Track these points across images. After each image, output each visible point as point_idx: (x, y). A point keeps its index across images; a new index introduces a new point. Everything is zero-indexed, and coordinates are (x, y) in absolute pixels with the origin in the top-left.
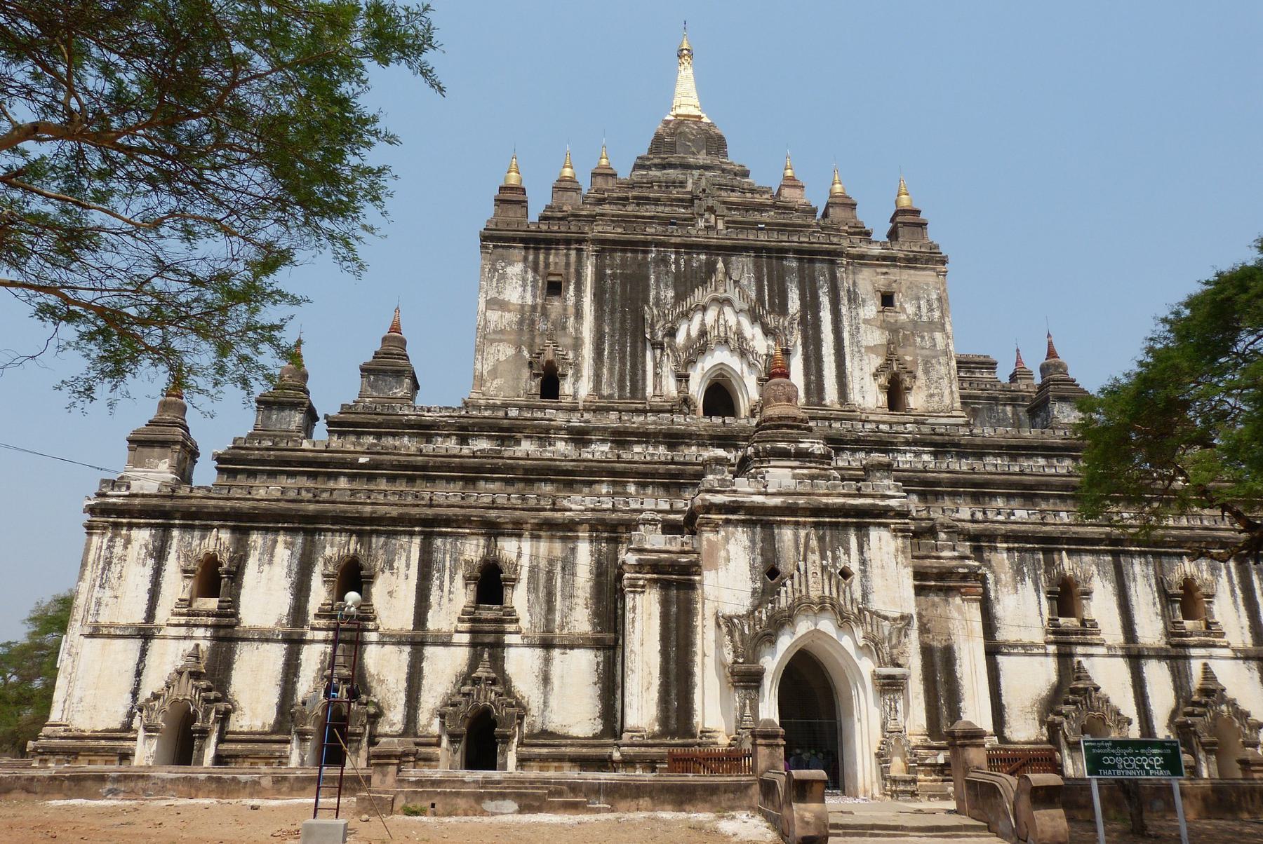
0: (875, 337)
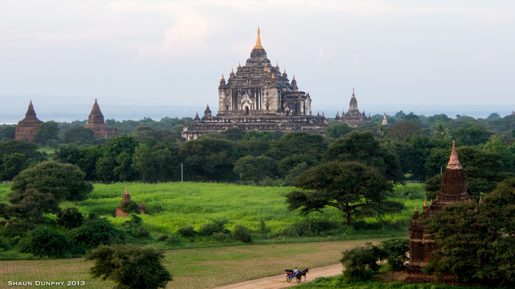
0: (265, 100)
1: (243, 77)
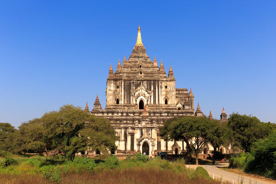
0: (164, 93)
1: (131, 70)
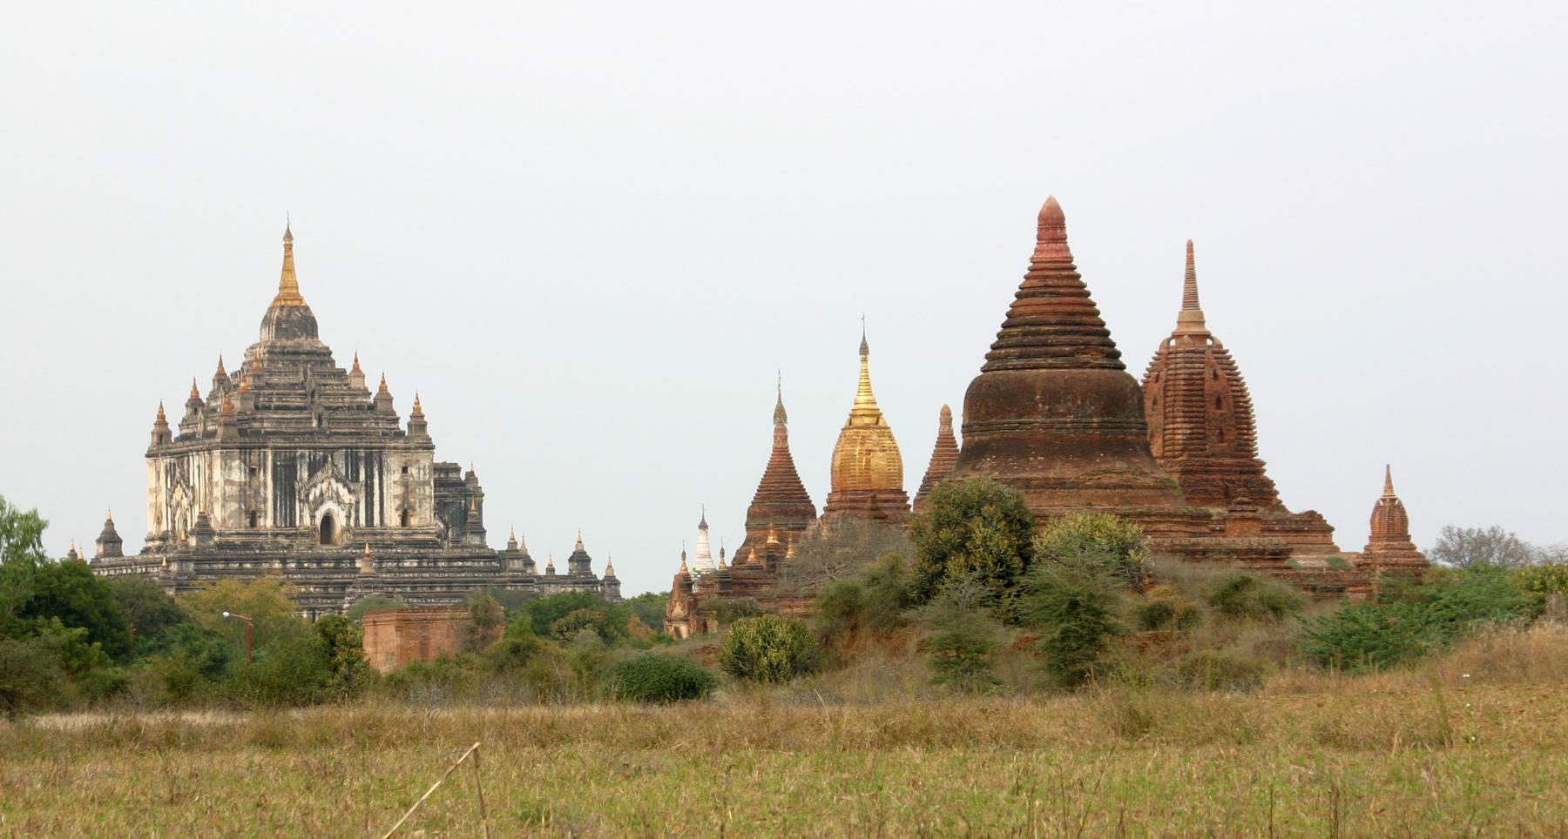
0: (399, 490)
